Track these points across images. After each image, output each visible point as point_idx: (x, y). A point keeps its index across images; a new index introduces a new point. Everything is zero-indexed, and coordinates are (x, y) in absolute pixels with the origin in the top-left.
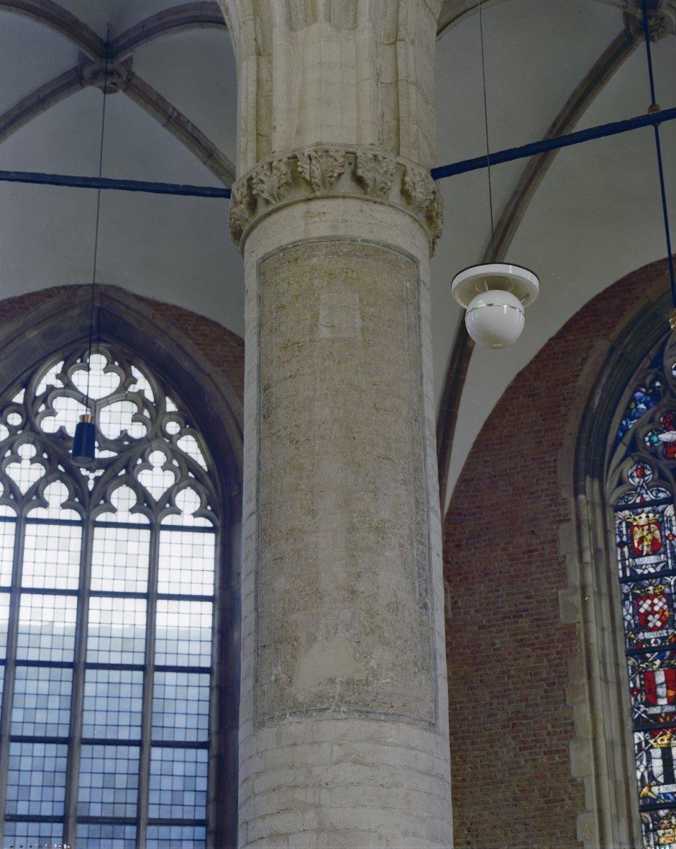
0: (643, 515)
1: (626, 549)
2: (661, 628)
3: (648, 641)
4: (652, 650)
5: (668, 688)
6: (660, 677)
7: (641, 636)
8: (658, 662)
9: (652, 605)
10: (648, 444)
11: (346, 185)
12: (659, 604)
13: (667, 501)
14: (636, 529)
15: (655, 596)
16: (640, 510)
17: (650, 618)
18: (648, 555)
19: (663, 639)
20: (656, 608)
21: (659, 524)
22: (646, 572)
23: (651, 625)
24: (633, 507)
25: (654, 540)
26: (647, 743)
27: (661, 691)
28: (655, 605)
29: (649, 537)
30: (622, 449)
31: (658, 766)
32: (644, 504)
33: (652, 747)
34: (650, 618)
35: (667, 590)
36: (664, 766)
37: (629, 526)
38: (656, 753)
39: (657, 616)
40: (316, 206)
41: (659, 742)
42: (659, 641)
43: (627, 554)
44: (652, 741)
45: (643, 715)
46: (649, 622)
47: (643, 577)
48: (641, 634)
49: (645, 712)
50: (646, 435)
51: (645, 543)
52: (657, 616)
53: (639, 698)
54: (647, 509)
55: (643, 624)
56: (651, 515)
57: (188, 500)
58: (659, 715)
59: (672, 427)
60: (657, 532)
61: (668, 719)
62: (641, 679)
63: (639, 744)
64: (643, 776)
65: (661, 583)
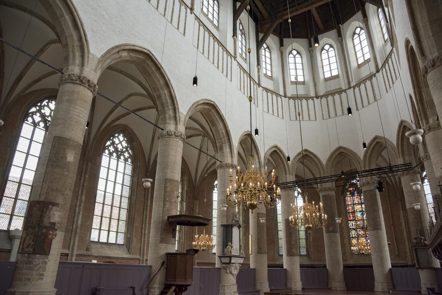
6: (351, 215)
11: (329, 190)
12: (351, 208)
13: (351, 196)
21: (351, 199)
24: (348, 197)
27: (351, 217)
30: (346, 190)
31: (351, 225)
38: (351, 223)
40: (327, 192)
55: (349, 210)
57: (300, 196)
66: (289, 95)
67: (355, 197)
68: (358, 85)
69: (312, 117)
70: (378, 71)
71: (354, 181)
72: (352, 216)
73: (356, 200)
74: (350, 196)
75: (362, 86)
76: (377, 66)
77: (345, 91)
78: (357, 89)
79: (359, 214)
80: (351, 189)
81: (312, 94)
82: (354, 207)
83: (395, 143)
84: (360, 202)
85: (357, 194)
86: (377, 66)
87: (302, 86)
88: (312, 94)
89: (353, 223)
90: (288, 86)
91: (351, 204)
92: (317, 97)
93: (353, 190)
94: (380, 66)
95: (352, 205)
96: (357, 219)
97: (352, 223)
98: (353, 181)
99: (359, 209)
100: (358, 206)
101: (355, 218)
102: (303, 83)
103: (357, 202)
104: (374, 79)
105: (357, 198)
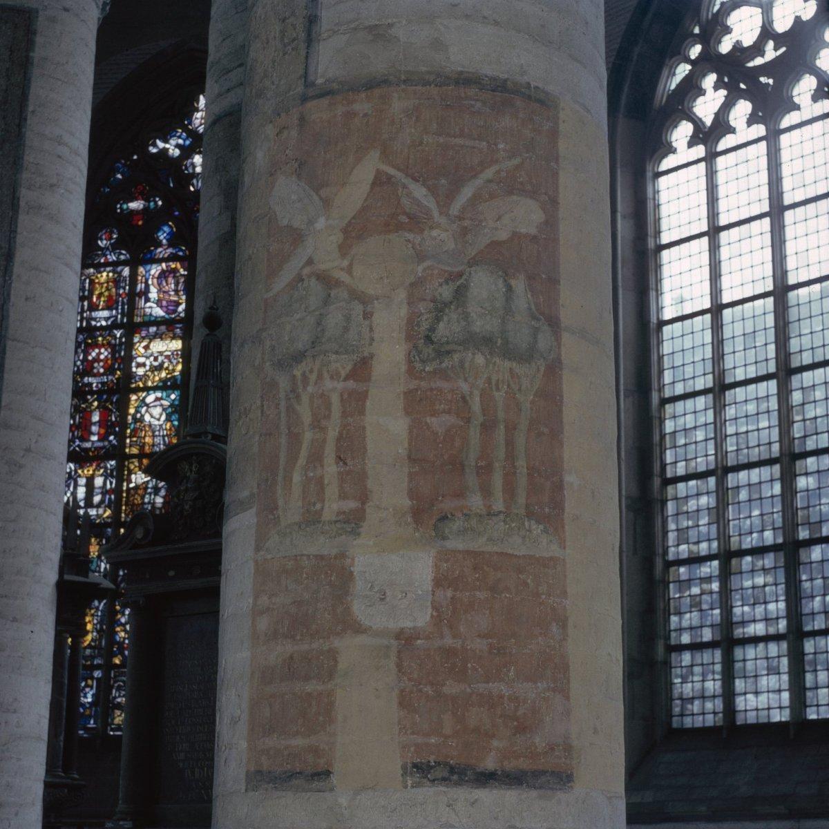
0: (105, 274)
1: (86, 303)
2: (103, 375)
3: (90, 384)
4: (92, 393)
5: (100, 427)
7: (86, 380)
8: (96, 404)
9: (100, 353)
10: (119, 211)
13: (125, 263)
14: (97, 286)
15: (103, 345)
16: (102, 269)
17: (96, 365)
18: (103, 309)
19: (103, 384)
20: (102, 357)
22: (99, 324)
23: (95, 371)
25: (110, 297)
26: (76, 471)
27: (94, 429)
28: (102, 353)
29: (106, 294)
32: (107, 264)
33: (80, 476)
34: (96, 365)
35: (113, 342)
36: (86, 493)
37: (92, 282)
38: (82, 481)
39: (101, 364)
41: (85, 472)
42: (100, 386)
43: (86, 308)
44: (80, 471)
45: (77, 449)
46: (94, 368)
47: (96, 328)
48: (86, 378)
49: (79, 446)
50: (118, 203)
51: (102, 299)
52: (101, 364)
53: (76, 433)
54: (108, 269)
56: (111, 274)
58: (90, 449)
59: (140, 197)
60: (114, 290)
61: (96, 453)
62: (80, 418)
63: (70, 474)
64: (68, 498)
65: (109, 335)
67: (155, 270)
71: (172, 147)
72: (101, 423)
73: (153, 294)
74: (115, 264)
79: (157, 411)
80: (135, 205)
82: (130, 346)
84: (181, 308)
85: (170, 245)
89: (99, 481)
91: (115, 326)
93: (146, 209)
95: (118, 333)
96: (135, 451)
97: (90, 480)
98: (161, 145)
99: (160, 368)
100: (158, 346)
101: (121, 437)
103: (159, 312)
105: (163, 275)
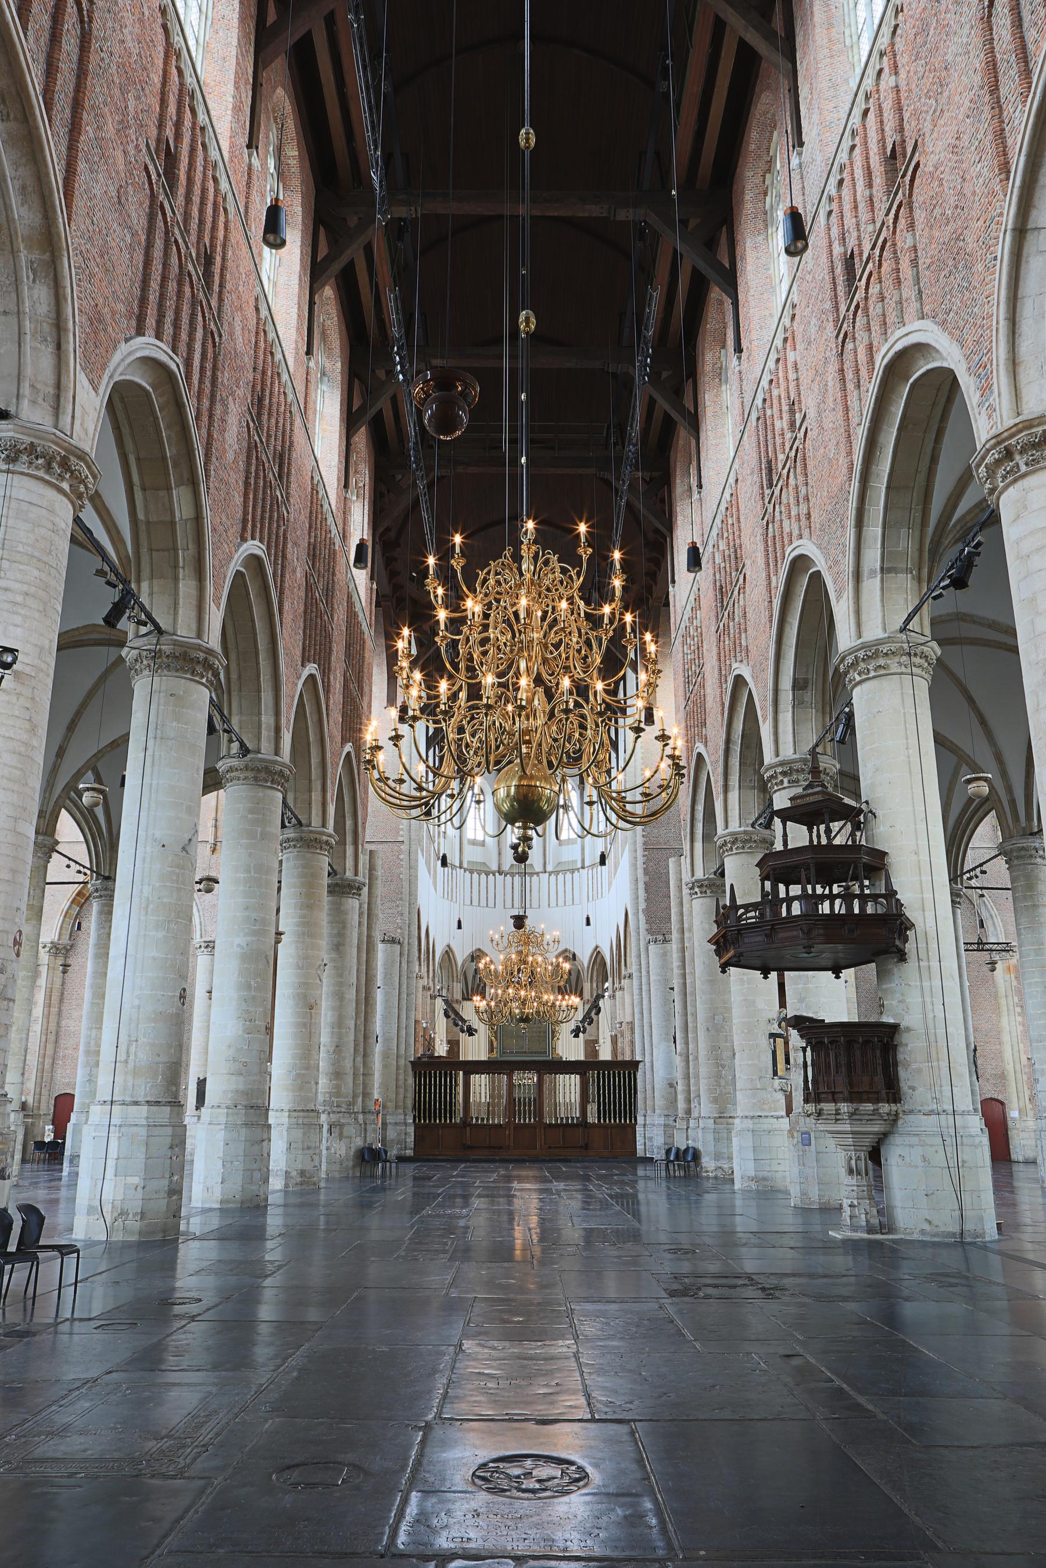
66: (465, 865)
68: (557, 873)
69: (491, 903)
70: (583, 868)
75: (561, 876)
76: (583, 861)
77: (538, 874)
78: (553, 877)
81: (495, 868)
83: (586, 965)
86: (583, 861)
87: (479, 848)
88: (494, 867)
90: (467, 848)
92: (500, 873)
94: (587, 864)
102: (483, 844)
104: (576, 874)
